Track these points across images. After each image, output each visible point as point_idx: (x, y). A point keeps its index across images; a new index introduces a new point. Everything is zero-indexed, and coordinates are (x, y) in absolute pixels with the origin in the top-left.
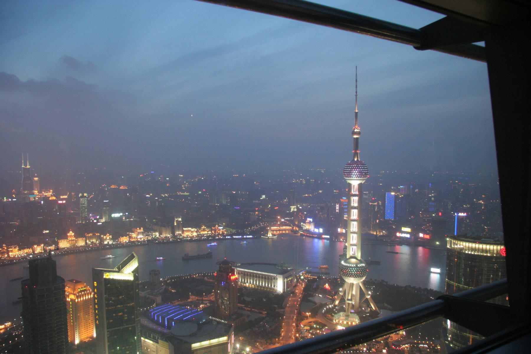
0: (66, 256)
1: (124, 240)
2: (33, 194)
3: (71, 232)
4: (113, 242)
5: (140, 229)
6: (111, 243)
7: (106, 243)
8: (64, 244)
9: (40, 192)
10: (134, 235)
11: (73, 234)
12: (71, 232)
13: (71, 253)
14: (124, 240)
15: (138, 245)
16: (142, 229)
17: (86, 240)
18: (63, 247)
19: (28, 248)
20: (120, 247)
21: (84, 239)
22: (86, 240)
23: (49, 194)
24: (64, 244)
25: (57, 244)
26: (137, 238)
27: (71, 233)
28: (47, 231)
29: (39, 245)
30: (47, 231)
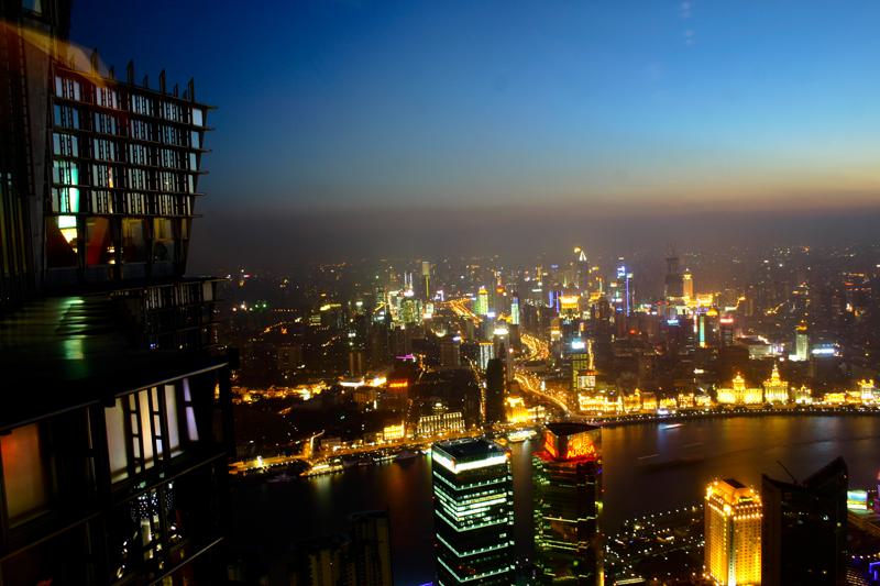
0: (729, 420)
1: (834, 399)
2: (682, 304)
3: (738, 377)
4: (814, 401)
5: (868, 382)
6: (809, 401)
7: (799, 401)
8: (726, 396)
9: (694, 298)
10: (854, 394)
11: (743, 381)
12: (738, 377)
13: (737, 415)
14: (834, 399)
15: (861, 414)
16: (871, 381)
17: (764, 394)
18: (725, 401)
19: (671, 397)
20: (825, 414)
21: (760, 391)
22: (764, 394)
23: (707, 301)
24: (726, 396)
25: (713, 395)
26: (860, 398)
27: (739, 380)
28: (701, 371)
29: (686, 394)
30: (701, 371)
